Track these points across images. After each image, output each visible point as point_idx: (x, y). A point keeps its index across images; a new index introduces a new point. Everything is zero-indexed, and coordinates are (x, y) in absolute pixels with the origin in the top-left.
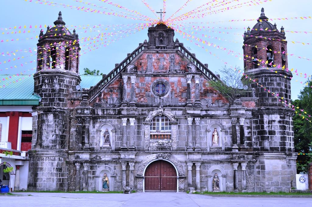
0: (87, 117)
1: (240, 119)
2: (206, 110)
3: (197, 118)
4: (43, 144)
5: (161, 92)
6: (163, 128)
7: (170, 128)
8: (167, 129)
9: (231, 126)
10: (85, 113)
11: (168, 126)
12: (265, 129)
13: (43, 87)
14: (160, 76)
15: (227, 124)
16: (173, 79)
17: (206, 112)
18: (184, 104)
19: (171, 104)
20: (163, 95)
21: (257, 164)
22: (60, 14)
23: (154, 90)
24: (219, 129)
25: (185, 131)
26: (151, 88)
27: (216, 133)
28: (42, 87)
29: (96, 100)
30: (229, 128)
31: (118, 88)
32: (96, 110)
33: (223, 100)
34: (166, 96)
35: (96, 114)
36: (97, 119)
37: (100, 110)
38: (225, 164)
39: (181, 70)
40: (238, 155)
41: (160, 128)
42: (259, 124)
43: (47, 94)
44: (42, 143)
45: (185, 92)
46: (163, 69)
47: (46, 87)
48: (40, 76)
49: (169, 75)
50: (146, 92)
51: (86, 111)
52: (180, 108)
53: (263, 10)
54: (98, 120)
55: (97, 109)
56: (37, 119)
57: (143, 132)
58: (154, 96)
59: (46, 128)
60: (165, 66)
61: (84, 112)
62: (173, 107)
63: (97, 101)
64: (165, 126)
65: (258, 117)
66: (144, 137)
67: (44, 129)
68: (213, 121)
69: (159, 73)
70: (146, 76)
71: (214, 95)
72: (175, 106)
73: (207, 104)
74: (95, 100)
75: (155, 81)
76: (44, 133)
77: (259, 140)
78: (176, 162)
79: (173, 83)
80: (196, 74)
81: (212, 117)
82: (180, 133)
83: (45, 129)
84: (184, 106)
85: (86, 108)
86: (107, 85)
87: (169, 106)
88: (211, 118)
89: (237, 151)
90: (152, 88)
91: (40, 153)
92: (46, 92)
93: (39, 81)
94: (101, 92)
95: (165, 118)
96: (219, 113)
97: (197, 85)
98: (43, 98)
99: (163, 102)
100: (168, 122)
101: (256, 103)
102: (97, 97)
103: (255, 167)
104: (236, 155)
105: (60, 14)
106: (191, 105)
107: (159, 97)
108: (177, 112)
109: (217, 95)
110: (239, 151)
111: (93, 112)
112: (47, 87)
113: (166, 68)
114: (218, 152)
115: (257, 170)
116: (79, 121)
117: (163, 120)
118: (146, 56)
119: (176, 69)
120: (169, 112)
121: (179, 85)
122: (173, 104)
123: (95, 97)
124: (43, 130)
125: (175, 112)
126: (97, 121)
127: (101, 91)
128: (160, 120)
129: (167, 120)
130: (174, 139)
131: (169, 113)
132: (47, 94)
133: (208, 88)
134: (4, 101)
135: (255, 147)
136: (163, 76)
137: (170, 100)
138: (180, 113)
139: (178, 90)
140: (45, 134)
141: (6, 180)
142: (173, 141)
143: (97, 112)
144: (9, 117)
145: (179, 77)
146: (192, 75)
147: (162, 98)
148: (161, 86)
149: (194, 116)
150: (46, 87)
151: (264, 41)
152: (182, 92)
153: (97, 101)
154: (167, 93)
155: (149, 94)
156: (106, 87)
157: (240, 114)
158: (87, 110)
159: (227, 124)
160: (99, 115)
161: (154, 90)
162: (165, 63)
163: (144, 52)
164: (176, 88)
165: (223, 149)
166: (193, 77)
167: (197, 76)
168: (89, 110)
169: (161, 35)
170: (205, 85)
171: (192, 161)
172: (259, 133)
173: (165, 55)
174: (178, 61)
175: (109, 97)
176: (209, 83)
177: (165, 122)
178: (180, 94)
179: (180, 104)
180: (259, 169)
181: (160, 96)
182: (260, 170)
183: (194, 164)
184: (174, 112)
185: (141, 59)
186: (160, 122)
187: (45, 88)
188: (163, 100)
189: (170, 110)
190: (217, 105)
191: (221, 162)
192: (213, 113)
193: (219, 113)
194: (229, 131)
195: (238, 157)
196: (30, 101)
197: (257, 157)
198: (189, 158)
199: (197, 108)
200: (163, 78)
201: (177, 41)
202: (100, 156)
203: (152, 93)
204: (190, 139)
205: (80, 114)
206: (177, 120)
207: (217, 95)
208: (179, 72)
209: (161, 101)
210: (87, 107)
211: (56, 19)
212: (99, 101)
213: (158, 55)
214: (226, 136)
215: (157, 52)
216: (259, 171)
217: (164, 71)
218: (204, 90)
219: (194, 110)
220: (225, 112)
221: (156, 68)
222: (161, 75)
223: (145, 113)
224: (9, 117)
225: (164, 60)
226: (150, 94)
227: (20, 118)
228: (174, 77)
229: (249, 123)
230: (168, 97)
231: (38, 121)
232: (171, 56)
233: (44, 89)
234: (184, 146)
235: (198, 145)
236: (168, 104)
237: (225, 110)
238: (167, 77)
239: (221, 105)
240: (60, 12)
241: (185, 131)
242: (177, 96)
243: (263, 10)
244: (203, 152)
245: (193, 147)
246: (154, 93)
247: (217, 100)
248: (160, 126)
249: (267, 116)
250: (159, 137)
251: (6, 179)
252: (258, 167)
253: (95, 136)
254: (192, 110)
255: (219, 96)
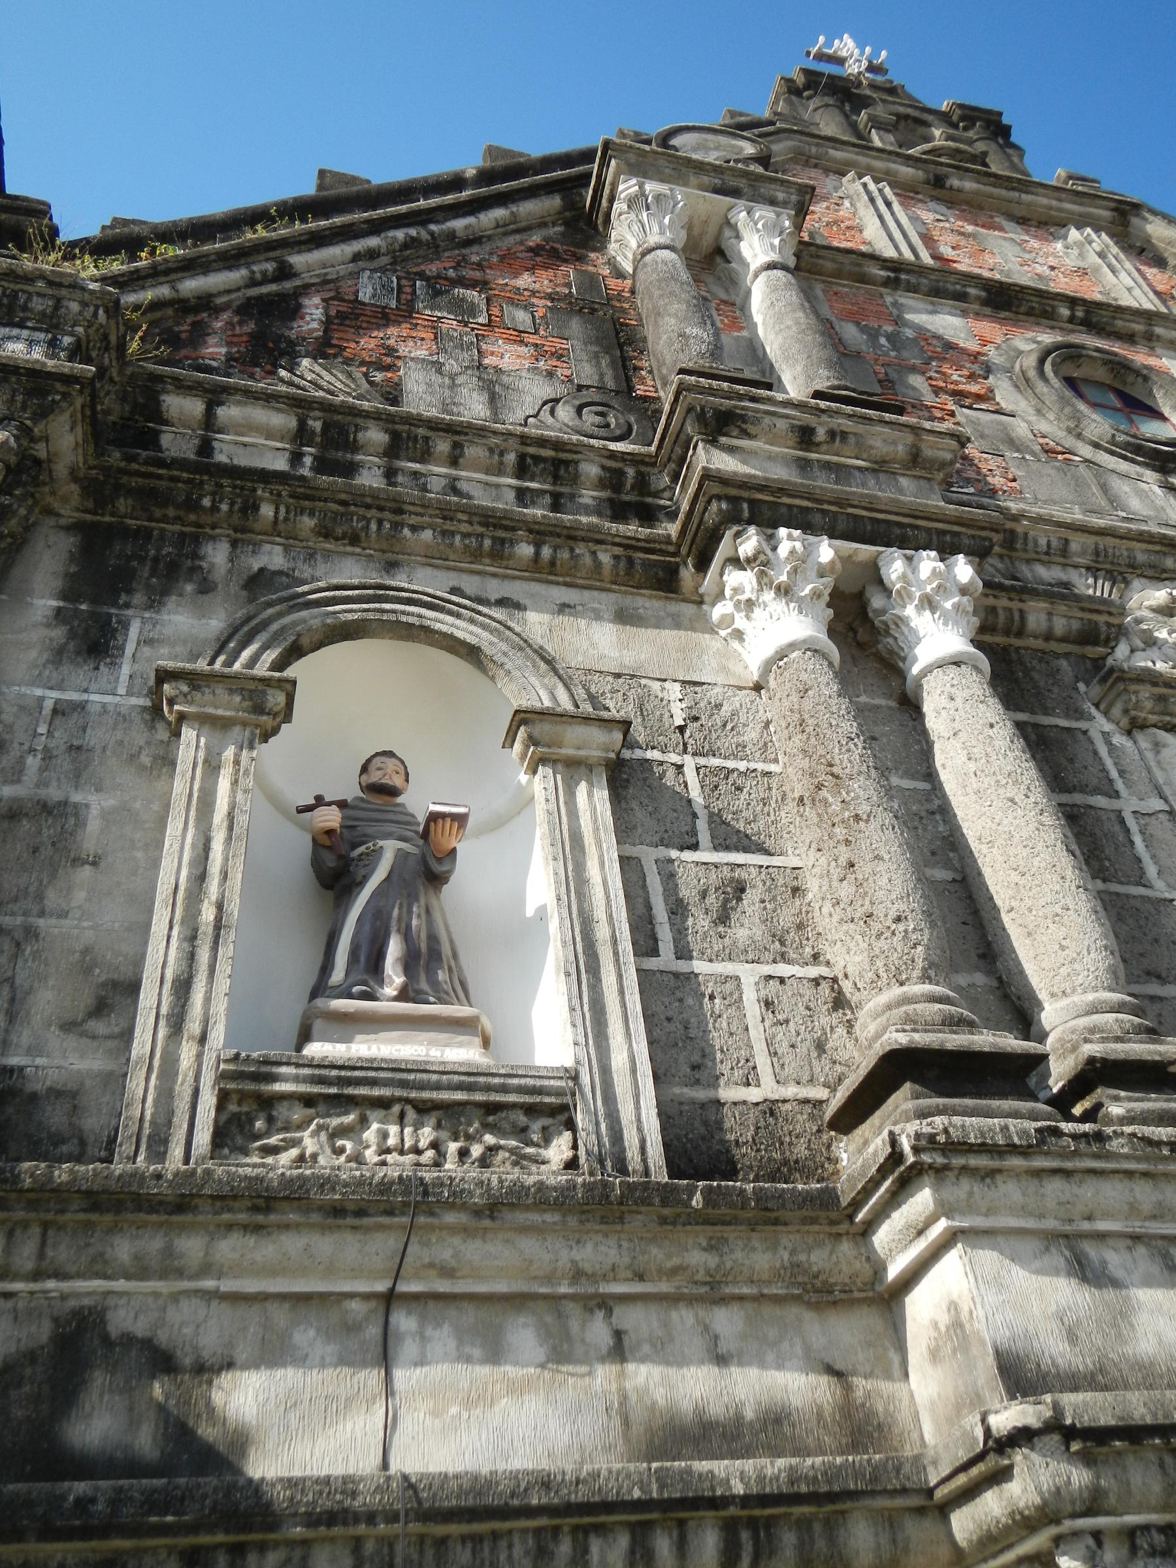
14: (1065, 312)
31: (550, 297)
32: (195, 407)
37: (260, 414)
49: (1158, 330)
54: (217, 555)
55: (215, 396)
70: (892, 284)
86: (400, 234)
94: (284, 272)
102: (205, 303)
123: (192, 285)
127: (298, 260)
156: (373, 242)
175: (422, 353)
202: (194, 1327)
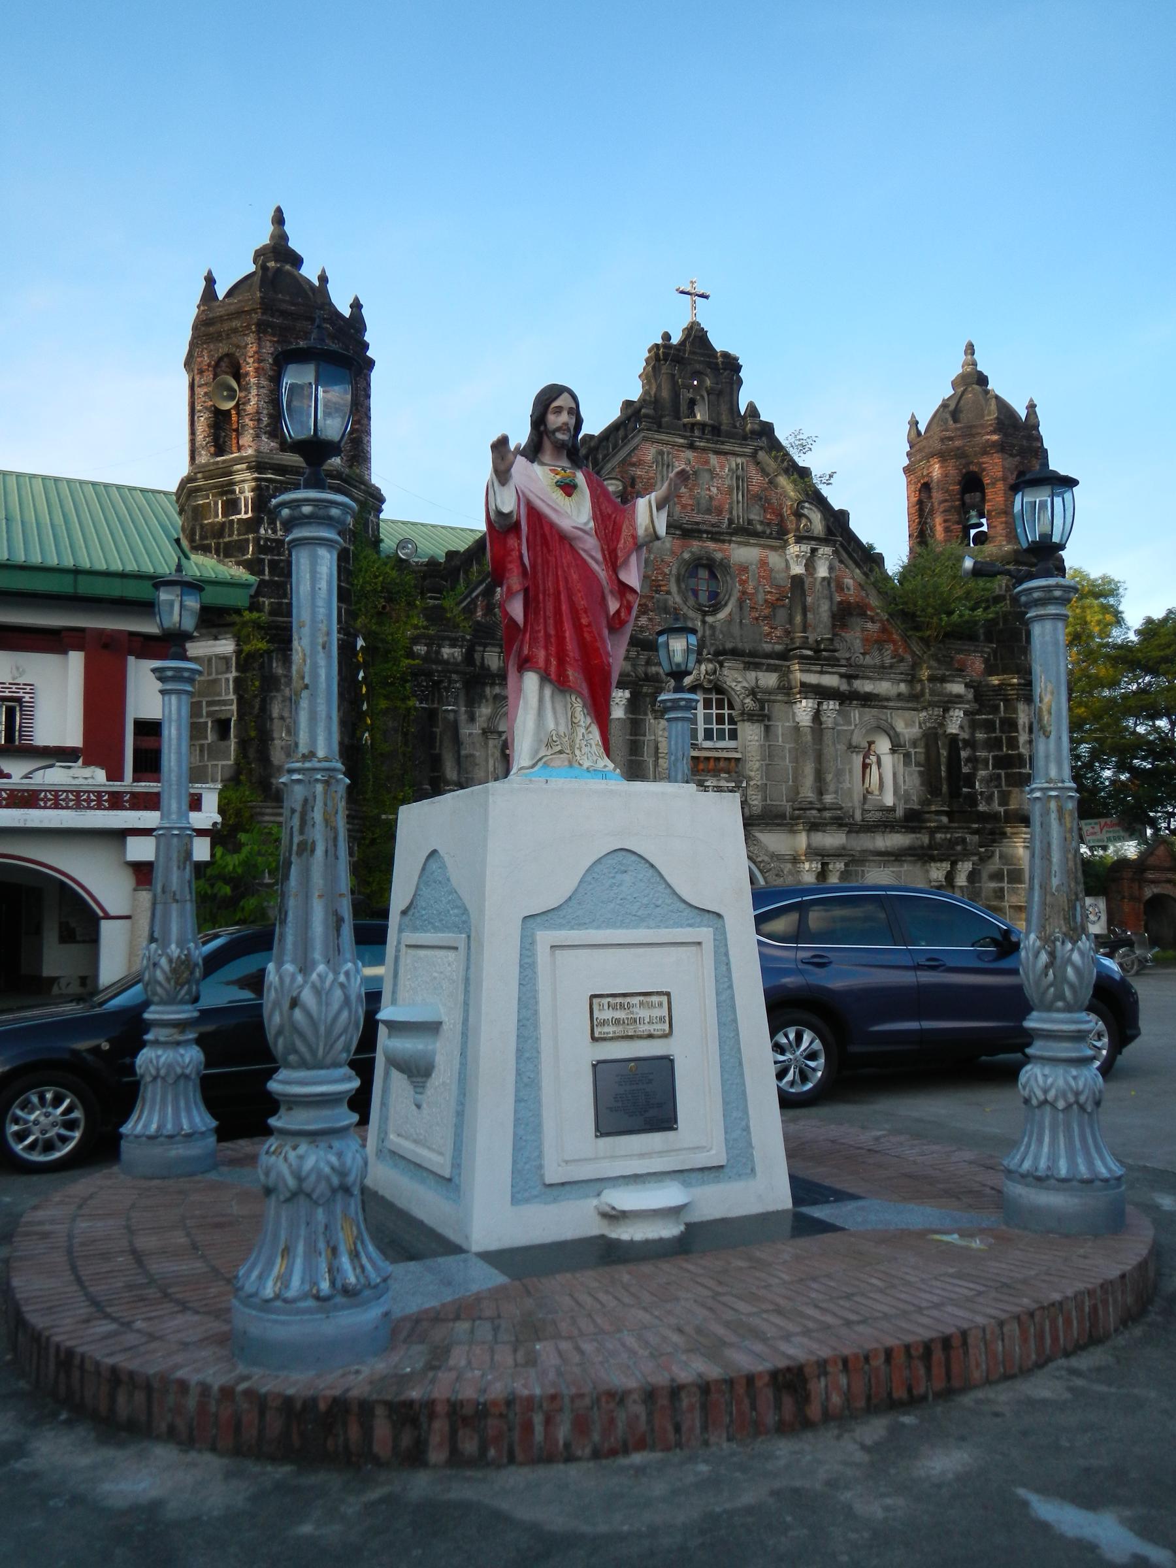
0: (454, 676)
1: (951, 713)
2: (849, 677)
3: (831, 702)
4: (274, 781)
5: (703, 597)
6: (708, 735)
7: (733, 735)
8: (721, 737)
9: (919, 735)
10: (446, 656)
11: (727, 727)
12: (1022, 750)
13: (262, 531)
15: (908, 726)
16: (743, 554)
17: (849, 684)
18: (778, 648)
19: (740, 645)
20: (716, 609)
21: (995, 865)
22: (279, 219)
23: (683, 586)
24: (883, 745)
25: (788, 746)
26: (673, 580)
27: (874, 758)
28: (257, 531)
29: (475, 608)
30: (914, 744)
32: (481, 649)
33: (894, 642)
34: (722, 615)
35: (478, 663)
36: (484, 684)
38: (906, 867)
39: (769, 524)
40: (949, 836)
41: (701, 734)
42: (998, 734)
43: (282, 565)
44: (270, 776)
45: (783, 606)
46: (708, 511)
47: (275, 532)
48: (238, 478)
50: (657, 592)
51: (446, 652)
52: (772, 662)
53: (970, 349)
54: (488, 690)
55: (485, 645)
56: (228, 670)
57: (652, 745)
58: (685, 609)
59: (286, 714)
60: (715, 503)
61: (438, 652)
62: (752, 659)
63: (479, 614)
64: (715, 727)
65: (996, 709)
66: (656, 764)
67: (275, 714)
68: (870, 714)
69: (697, 523)
71: (869, 625)
72: (753, 654)
73: (847, 655)
74: (469, 611)
75: (686, 556)
76: (276, 735)
77: (999, 786)
78: (766, 859)
79: (744, 569)
80: (824, 541)
81: (867, 700)
82: (769, 754)
83: (282, 718)
84: (784, 656)
85: (450, 639)
87: (735, 653)
88: (864, 706)
89: (945, 819)
90: (678, 581)
91: (267, 818)
92: (279, 555)
93: (232, 506)
95: (714, 697)
96: (884, 687)
97: (825, 583)
98: (267, 578)
99: (713, 635)
100: (726, 712)
101: (986, 661)
102: (477, 597)
103: (985, 875)
104: (943, 836)
105: (279, 219)
106: (809, 653)
107: (700, 617)
108: (760, 674)
109: (878, 625)
110: (950, 821)
111: (469, 657)
112: (280, 533)
113: (719, 512)
114: (886, 823)
115: (993, 885)
116: (422, 691)
117: (707, 704)
118: (649, 452)
119: (752, 517)
120: (736, 675)
121: (764, 578)
122: (747, 647)
123: (474, 594)
124: (272, 719)
125: (753, 674)
126: (482, 696)
128: (700, 705)
129: (720, 706)
130: (752, 774)
131: (737, 679)
132: (282, 565)
133: (852, 599)
134: (80, 577)
135: (982, 808)
136: (716, 537)
137: (736, 630)
138: (769, 680)
139: (760, 597)
140: (281, 739)
141: (78, 942)
142: (752, 783)
143: (483, 658)
144: (76, 660)
145: (764, 546)
146: (813, 544)
147: (710, 619)
148: (703, 574)
149: (821, 693)
150: (275, 532)
151: (986, 457)
152: (773, 606)
153: (479, 614)
154: (726, 605)
155: (666, 601)
157: (951, 695)
158: (453, 646)
159: (908, 726)
160: (488, 669)
161: (683, 586)
162: (714, 490)
163: (645, 439)
164: (755, 588)
165: (900, 813)
166: (813, 551)
167: (825, 551)
168: (461, 647)
169: (692, 378)
170: (840, 587)
171: (823, 856)
172: (1000, 762)
173: (714, 460)
174: (756, 489)
176: (853, 578)
177: (714, 711)
178: (766, 612)
179: (767, 647)
180: (1001, 880)
181: (705, 614)
182: (1005, 885)
183: (824, 865)
184: (751, 675)
185: (634, 465)
186: (701, 711)
187: (273, 536)
188: (712, 627)
189: (742, 666)
190: (877, 661)
191: (896, 860)
192: (867, 687)
193: (884, 687)
194: (912, 751)
195: (950, 840)
196: (225, 590)
197: (994, 841)
198: (809, 846)
199: (833, 666)
200: (711, 545)
201: (753, 411)
203: (678, 599)
204: (808, 781)
205: (426, 658)
206: (762, 703)
207: (878, 625)
208: (759, 528)
209: (708, 633)
210: (453, 635)
211: (263, 237)
212: (484, 615)
213: (690, 454)
214: (908, 769)
215: (691, 446)
216: (1002, 889)
217: (713, 519)
218: (840, 603)
219: (822, 672)
220: (903, 687)
221: (684, 507)
222: (707, 532)
223: (658, 674)
224: (76, 660)
225: (712, 478)
226: (670, 603)
227: (131, 659)
228: (747, 544)
229: (966, 729)
230: (729, 621)
231: (237, 681)
232: (734, 466)
233: (267, 539)
234: (784, 803)
235: (828, 799)
236: (729, 646)
237: (902, 681)
238: (723, 541)
239: (888, 661)
240: (279, 211)
241: (788, 746)
242: (757, 619)
243: (970, 349)
244: (841, 822)
245: (818, 806)
246: (685, 602)
247: (876, 641)
248: (701, 726)
249: (1026, 707)
250: (701, 766)
251: (78, 938)
252: (997, 876)
253: (478, 754)
254: (816, 672)
255: (884, 630)
